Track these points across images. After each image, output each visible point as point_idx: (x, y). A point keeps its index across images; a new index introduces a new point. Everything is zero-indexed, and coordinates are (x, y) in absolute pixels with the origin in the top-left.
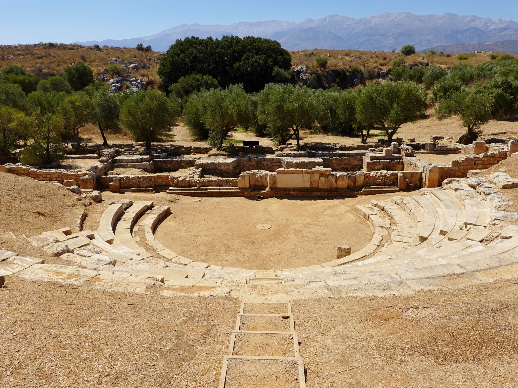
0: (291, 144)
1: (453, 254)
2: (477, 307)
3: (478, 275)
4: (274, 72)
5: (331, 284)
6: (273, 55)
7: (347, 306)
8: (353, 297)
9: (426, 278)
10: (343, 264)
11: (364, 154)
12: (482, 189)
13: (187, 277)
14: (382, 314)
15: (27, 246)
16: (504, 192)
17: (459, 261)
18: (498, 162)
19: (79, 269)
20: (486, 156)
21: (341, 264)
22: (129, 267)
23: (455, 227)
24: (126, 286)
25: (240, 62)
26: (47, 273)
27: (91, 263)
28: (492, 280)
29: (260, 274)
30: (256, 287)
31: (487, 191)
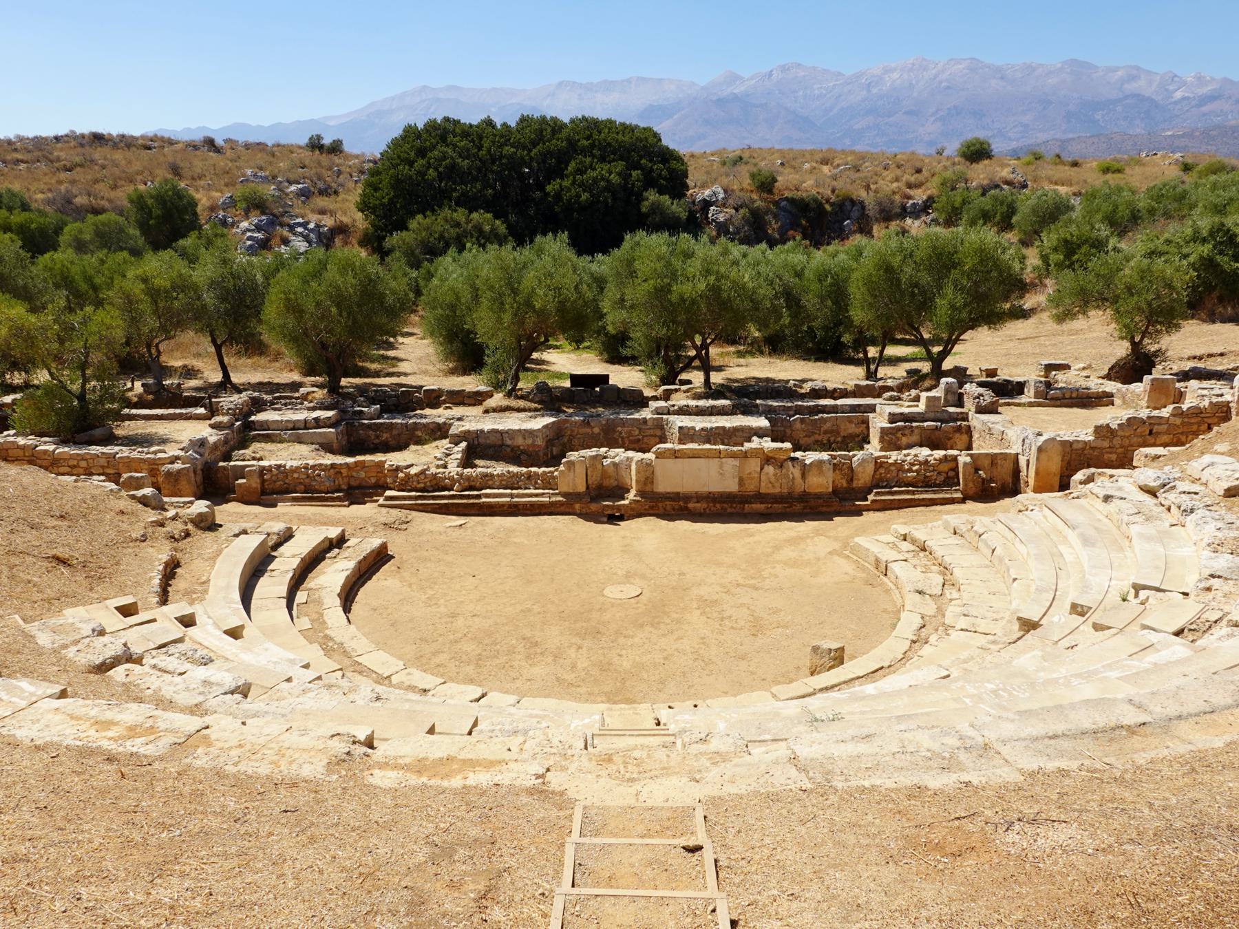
0: (689, 382)
1: (1109, 667)
2: (1190, 820)
3: (1184, 728)
4: (646, 203)
5: (804, 752)
6: (643, 161)
7: (850, 816)
8: (863, 790)
9: (1050, 738)
10: (827, 689)
11: (872, 408)
12: (1172, 497)
13: (431, 731)
14: (944, 838)
15: (24, 646)
16: (1229, 504)
17: (1128, 690)
18: (1210, 428)
19: (156, 713)
20: (1178, 413)
21: (821, 690)
22: (283, 703)
23: (1109, 595)
24: (276, 758)
25: (562, 178)
26: (74, 722)
27: (187, 689)
28: (1219, 743)
29: (618, 716)
30: (609, 759)
31: (1186, 501)
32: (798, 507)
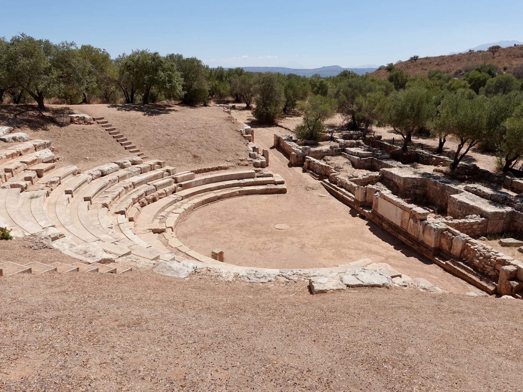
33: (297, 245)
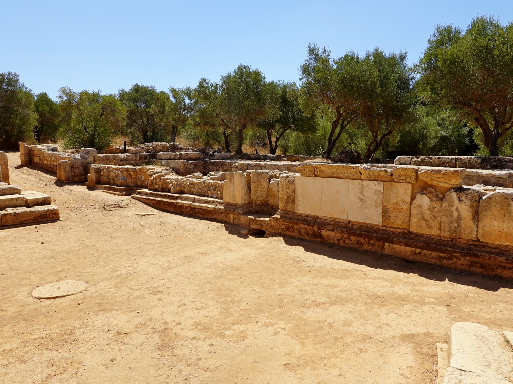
32: (462, 261)
33: (139, 338)
